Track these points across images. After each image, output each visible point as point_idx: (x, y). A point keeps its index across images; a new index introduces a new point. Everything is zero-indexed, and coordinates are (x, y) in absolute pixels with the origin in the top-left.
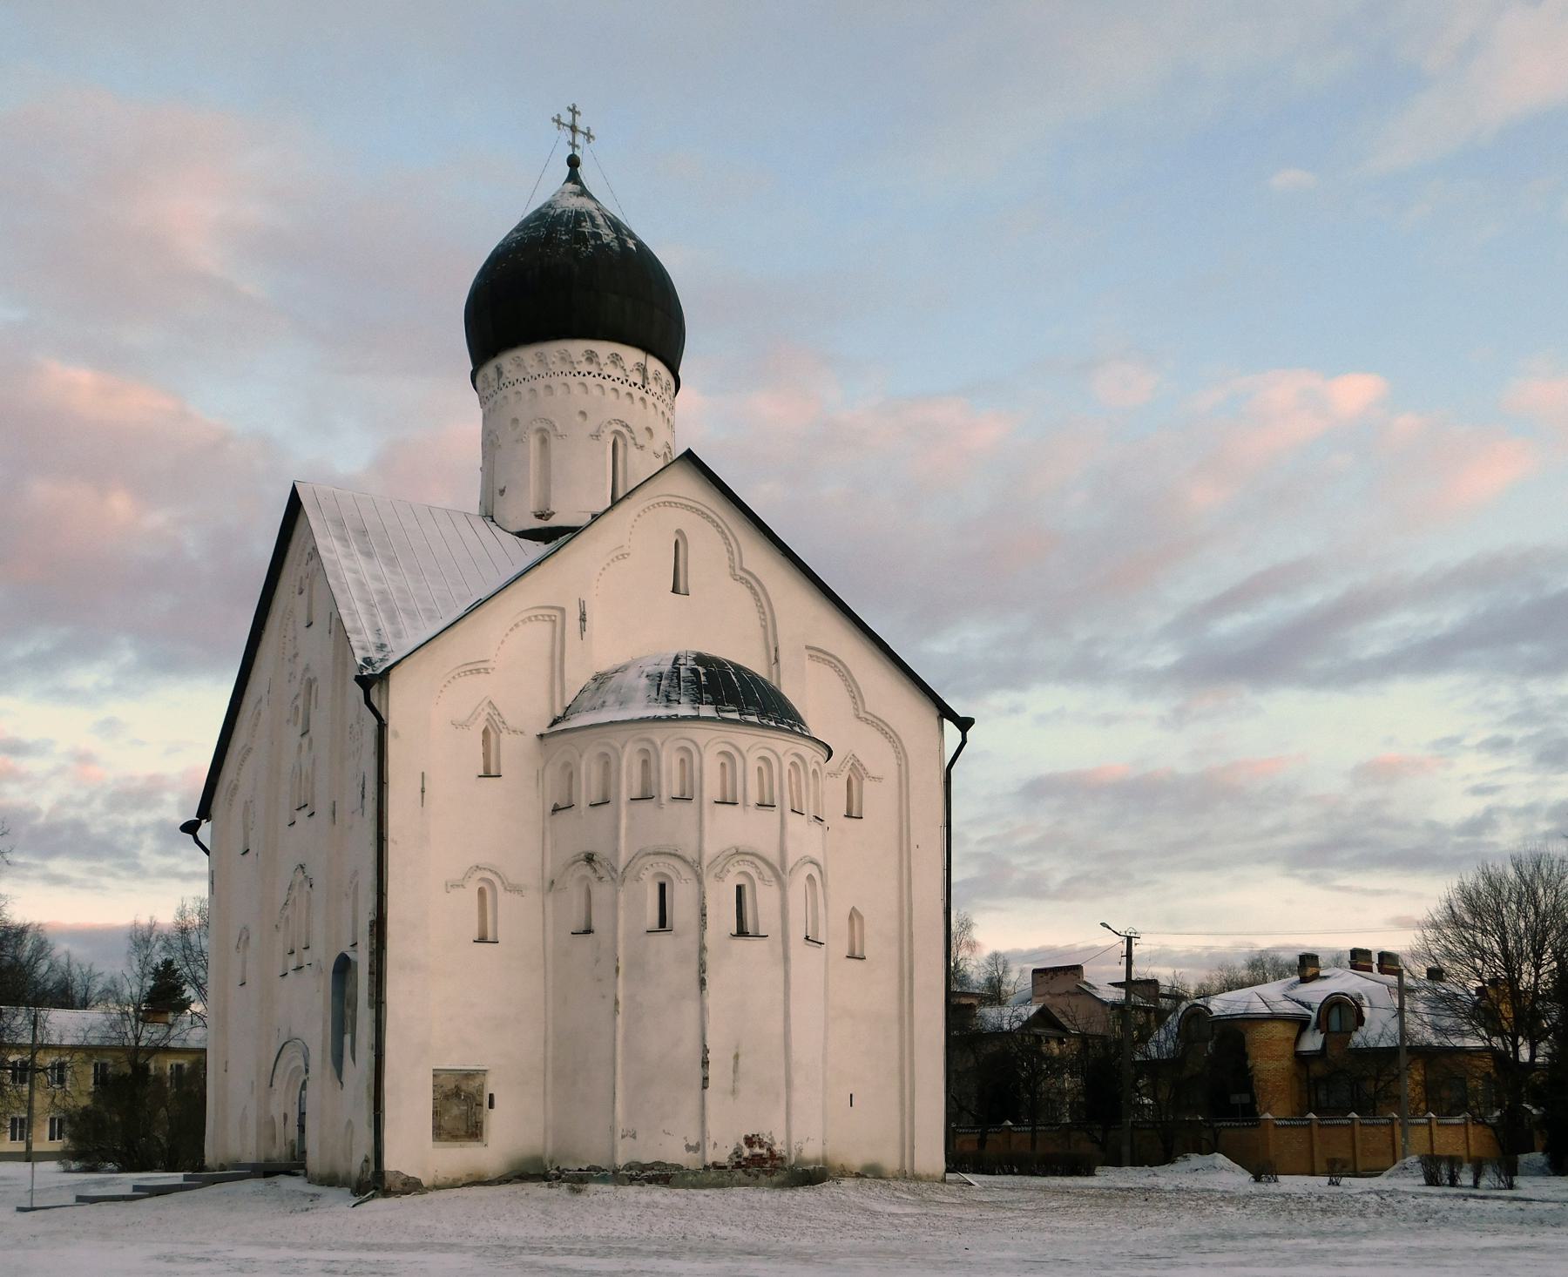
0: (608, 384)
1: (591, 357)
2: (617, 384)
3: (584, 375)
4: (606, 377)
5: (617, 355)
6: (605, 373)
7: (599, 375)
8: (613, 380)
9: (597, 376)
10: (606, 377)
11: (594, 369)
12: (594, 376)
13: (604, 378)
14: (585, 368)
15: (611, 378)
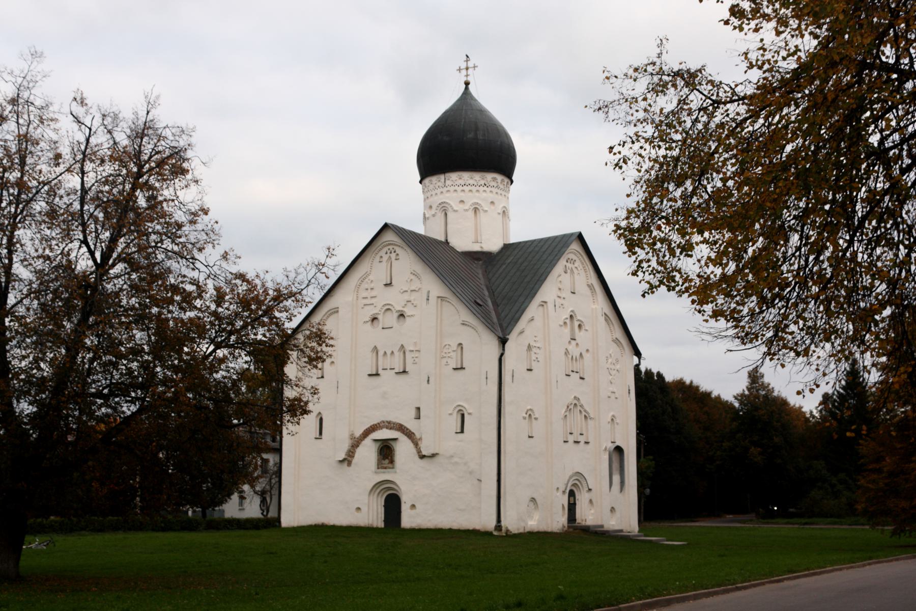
0: (499, 191)
1: (494, 179)
14: (493, 184)
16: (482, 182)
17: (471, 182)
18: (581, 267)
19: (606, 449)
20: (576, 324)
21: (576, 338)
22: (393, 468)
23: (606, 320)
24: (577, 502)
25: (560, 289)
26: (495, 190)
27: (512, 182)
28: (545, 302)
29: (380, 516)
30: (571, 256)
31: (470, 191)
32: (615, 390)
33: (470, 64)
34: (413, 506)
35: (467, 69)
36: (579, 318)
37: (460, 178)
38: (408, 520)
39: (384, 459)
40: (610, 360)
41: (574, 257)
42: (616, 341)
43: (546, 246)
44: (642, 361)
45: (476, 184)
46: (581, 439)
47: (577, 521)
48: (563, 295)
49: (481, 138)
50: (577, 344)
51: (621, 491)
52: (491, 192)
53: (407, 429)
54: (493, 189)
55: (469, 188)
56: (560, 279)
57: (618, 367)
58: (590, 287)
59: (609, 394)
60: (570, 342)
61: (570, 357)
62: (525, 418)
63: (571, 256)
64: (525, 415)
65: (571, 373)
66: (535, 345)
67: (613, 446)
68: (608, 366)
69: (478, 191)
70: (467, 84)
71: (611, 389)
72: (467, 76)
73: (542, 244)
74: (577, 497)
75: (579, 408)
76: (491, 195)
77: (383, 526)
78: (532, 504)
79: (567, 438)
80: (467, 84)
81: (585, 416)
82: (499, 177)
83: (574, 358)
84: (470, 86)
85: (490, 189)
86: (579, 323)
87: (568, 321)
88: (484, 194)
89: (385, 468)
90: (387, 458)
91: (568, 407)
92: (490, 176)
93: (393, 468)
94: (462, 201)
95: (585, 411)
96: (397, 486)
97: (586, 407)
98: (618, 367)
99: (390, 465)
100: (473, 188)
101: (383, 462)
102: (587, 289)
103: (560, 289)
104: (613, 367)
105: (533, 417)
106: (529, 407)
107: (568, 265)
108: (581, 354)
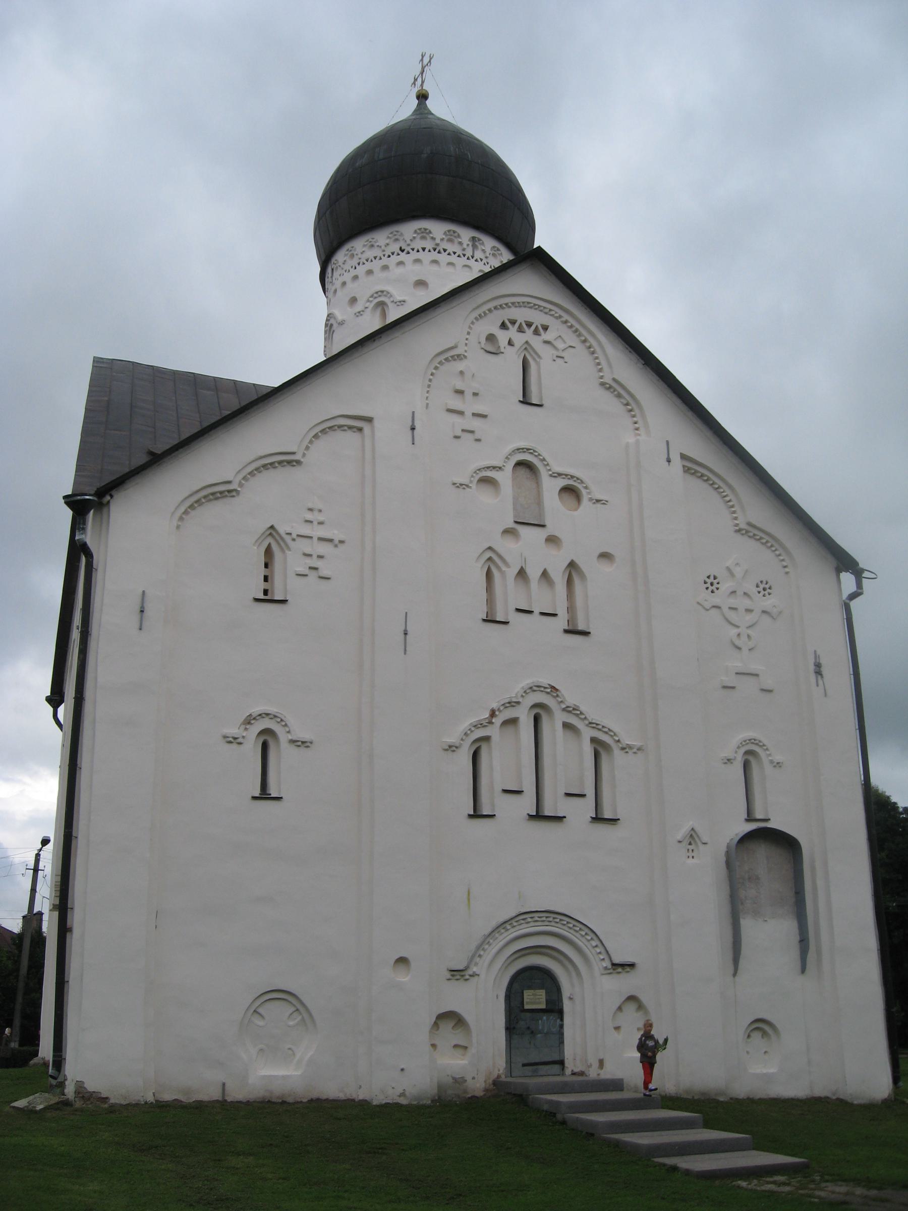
0: (443, 258)
1: (424, 234)
2: (453, 258)
3: (418, 251)
4: (442, 251)
5: (454, 232)
6: (440, 248)
7: (435, 250)
8: (449, 254)
9: (432, 250)
10: (442, 251)
11: (429, 245)
12: (429, 251)
13: (439, 252)
14: (419, 244)
15: (447, 252)
16: (395, 247)
17: (370, 254)
18: (572, 340)
19: (692, 837)
20: (551, 487)
21: (547, 523)
23: (687, 470)
24: (567, 1006)
25: (460, 392)
26: (426, 257)
28: (369, 420)
30: (521, 315)
31: (370, 272)
32: (754, 667)
33: (426, 60)
35: (422, 73)
36: (557, 469)
37: (352, 256)
40: (726, 586)
41: (539, 318)
42: (751, 531)
44: (865, 582)
45: (380, 254)
46: (563, 807)
47: (570, 1066)
48: (470, 406)
49: (381, 157)
50: (552, 540)
51: (803, 970)
52: (417, 261)
54: (421, 255)
55: (368, 266)
56: (460, 366)
57: (768, 603)
58: (613, 388)
59: (730, 680)
60: (507, 532)
61: (512, 572)
62: (233, 740)
63: (521, 315)
64: (234, 731)
65: (514, 617)
66: (306, 530)
67: (753, 826)
68: (715, 599)
69: (385, 268)
70: (422, 97)
71: (738, 665)
72: (423, 82)
74: (566, 994)
75: (560, 717)
76: (417, 267)
78: (278, 1011)
79: (493, 805)
80: (422, 97)
81: (594, 740)
82: (438, 229)
83: (534, 573)
84: (429, 103)
85: (414, 255)
86: (562, 482)
87: (505, 478)
88: (400, 270)
91: (493, 714)
92: (409, 229)
94: (353, 300)
95: (592, 725)
97: (593, 716)
98: (768, 603)
100: (376, 265)
102: (607, 396)
103: (460, 392)
104: (742, 603)
105: (283, 737)
106: (256, 710)
108: (572, 565)
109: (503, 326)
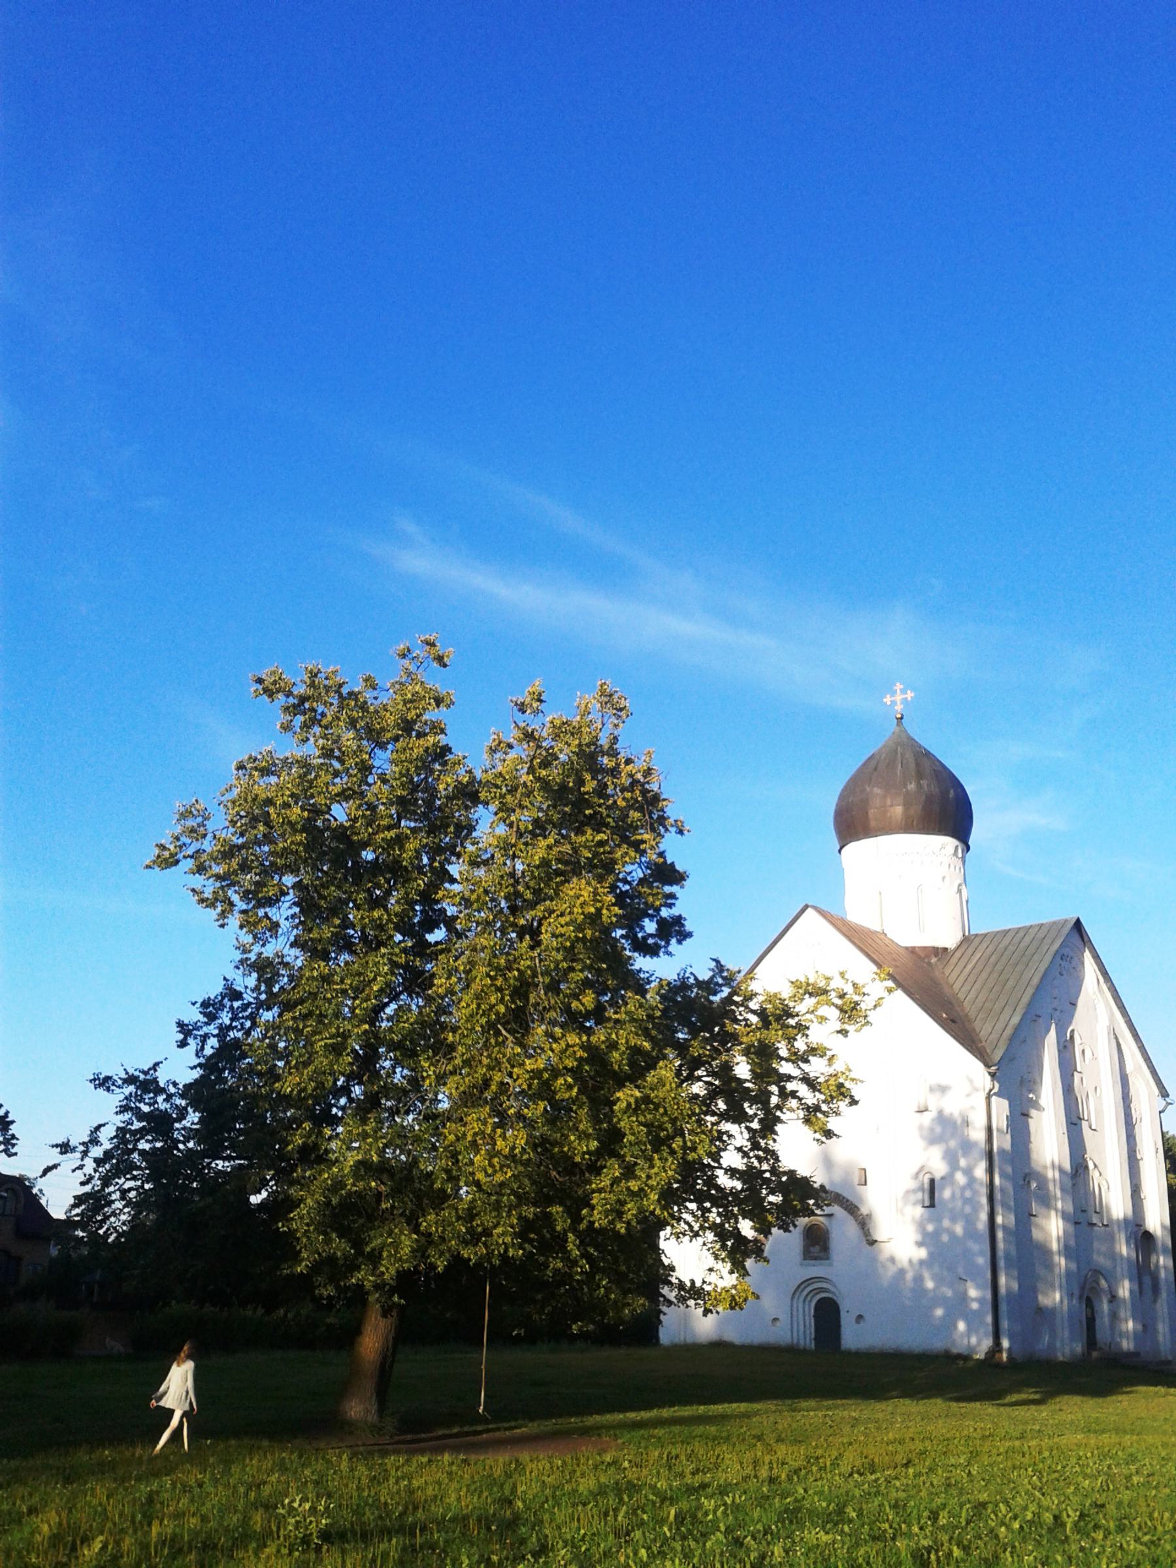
22: (828, 1259)
27: (968, 848)
29: (808, 1332)
34: (860, 1318)
38: (852, 1337)
39: (813, 1245)
43: (1027, 939)
53: (848, 1201)
73: (1021, 934)
77: (813, 1346)
89: (816, 1259)
90: (817, 1243)
93: (828, 1259)
96: (835, 1286)
99: (822, 1254)
101: (812, 1249)
107: (1063, 963)
109: (1062, 959)
